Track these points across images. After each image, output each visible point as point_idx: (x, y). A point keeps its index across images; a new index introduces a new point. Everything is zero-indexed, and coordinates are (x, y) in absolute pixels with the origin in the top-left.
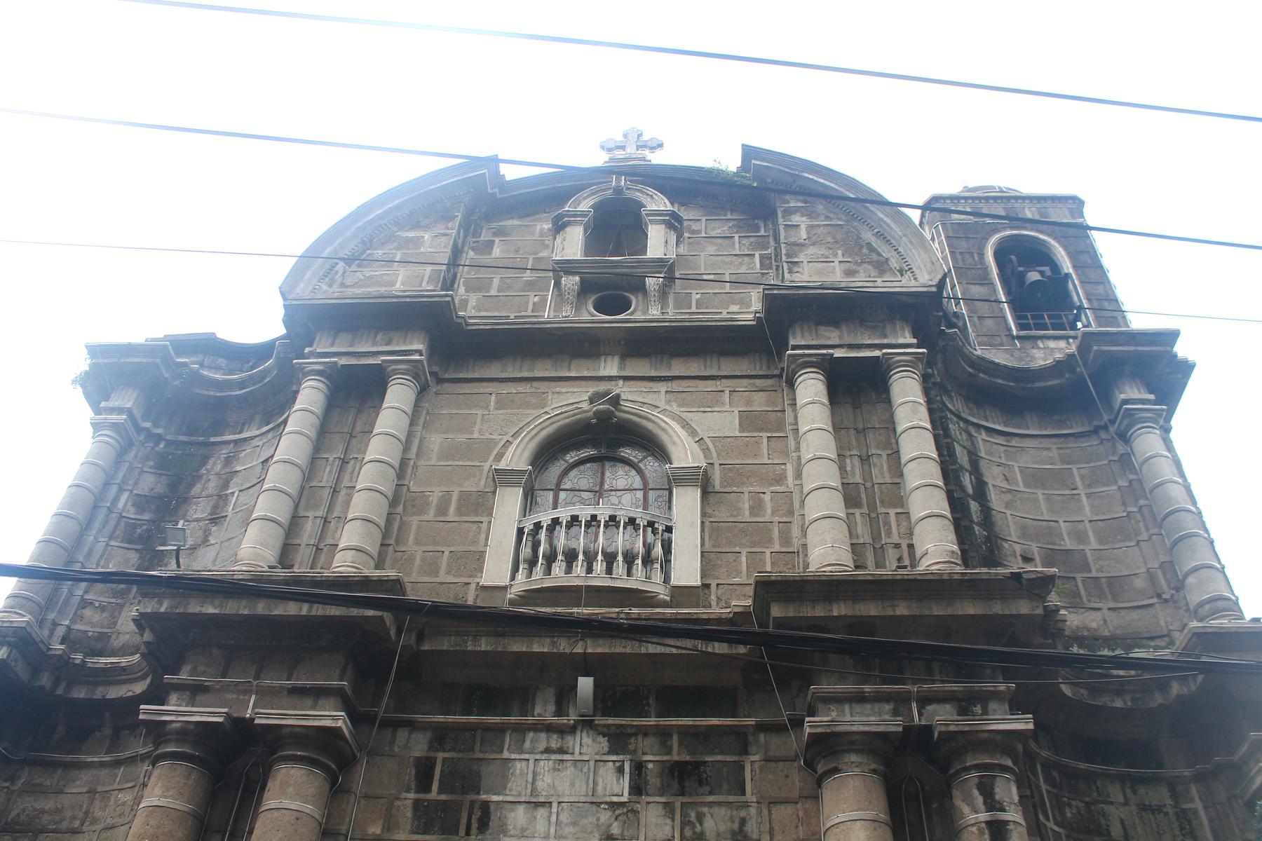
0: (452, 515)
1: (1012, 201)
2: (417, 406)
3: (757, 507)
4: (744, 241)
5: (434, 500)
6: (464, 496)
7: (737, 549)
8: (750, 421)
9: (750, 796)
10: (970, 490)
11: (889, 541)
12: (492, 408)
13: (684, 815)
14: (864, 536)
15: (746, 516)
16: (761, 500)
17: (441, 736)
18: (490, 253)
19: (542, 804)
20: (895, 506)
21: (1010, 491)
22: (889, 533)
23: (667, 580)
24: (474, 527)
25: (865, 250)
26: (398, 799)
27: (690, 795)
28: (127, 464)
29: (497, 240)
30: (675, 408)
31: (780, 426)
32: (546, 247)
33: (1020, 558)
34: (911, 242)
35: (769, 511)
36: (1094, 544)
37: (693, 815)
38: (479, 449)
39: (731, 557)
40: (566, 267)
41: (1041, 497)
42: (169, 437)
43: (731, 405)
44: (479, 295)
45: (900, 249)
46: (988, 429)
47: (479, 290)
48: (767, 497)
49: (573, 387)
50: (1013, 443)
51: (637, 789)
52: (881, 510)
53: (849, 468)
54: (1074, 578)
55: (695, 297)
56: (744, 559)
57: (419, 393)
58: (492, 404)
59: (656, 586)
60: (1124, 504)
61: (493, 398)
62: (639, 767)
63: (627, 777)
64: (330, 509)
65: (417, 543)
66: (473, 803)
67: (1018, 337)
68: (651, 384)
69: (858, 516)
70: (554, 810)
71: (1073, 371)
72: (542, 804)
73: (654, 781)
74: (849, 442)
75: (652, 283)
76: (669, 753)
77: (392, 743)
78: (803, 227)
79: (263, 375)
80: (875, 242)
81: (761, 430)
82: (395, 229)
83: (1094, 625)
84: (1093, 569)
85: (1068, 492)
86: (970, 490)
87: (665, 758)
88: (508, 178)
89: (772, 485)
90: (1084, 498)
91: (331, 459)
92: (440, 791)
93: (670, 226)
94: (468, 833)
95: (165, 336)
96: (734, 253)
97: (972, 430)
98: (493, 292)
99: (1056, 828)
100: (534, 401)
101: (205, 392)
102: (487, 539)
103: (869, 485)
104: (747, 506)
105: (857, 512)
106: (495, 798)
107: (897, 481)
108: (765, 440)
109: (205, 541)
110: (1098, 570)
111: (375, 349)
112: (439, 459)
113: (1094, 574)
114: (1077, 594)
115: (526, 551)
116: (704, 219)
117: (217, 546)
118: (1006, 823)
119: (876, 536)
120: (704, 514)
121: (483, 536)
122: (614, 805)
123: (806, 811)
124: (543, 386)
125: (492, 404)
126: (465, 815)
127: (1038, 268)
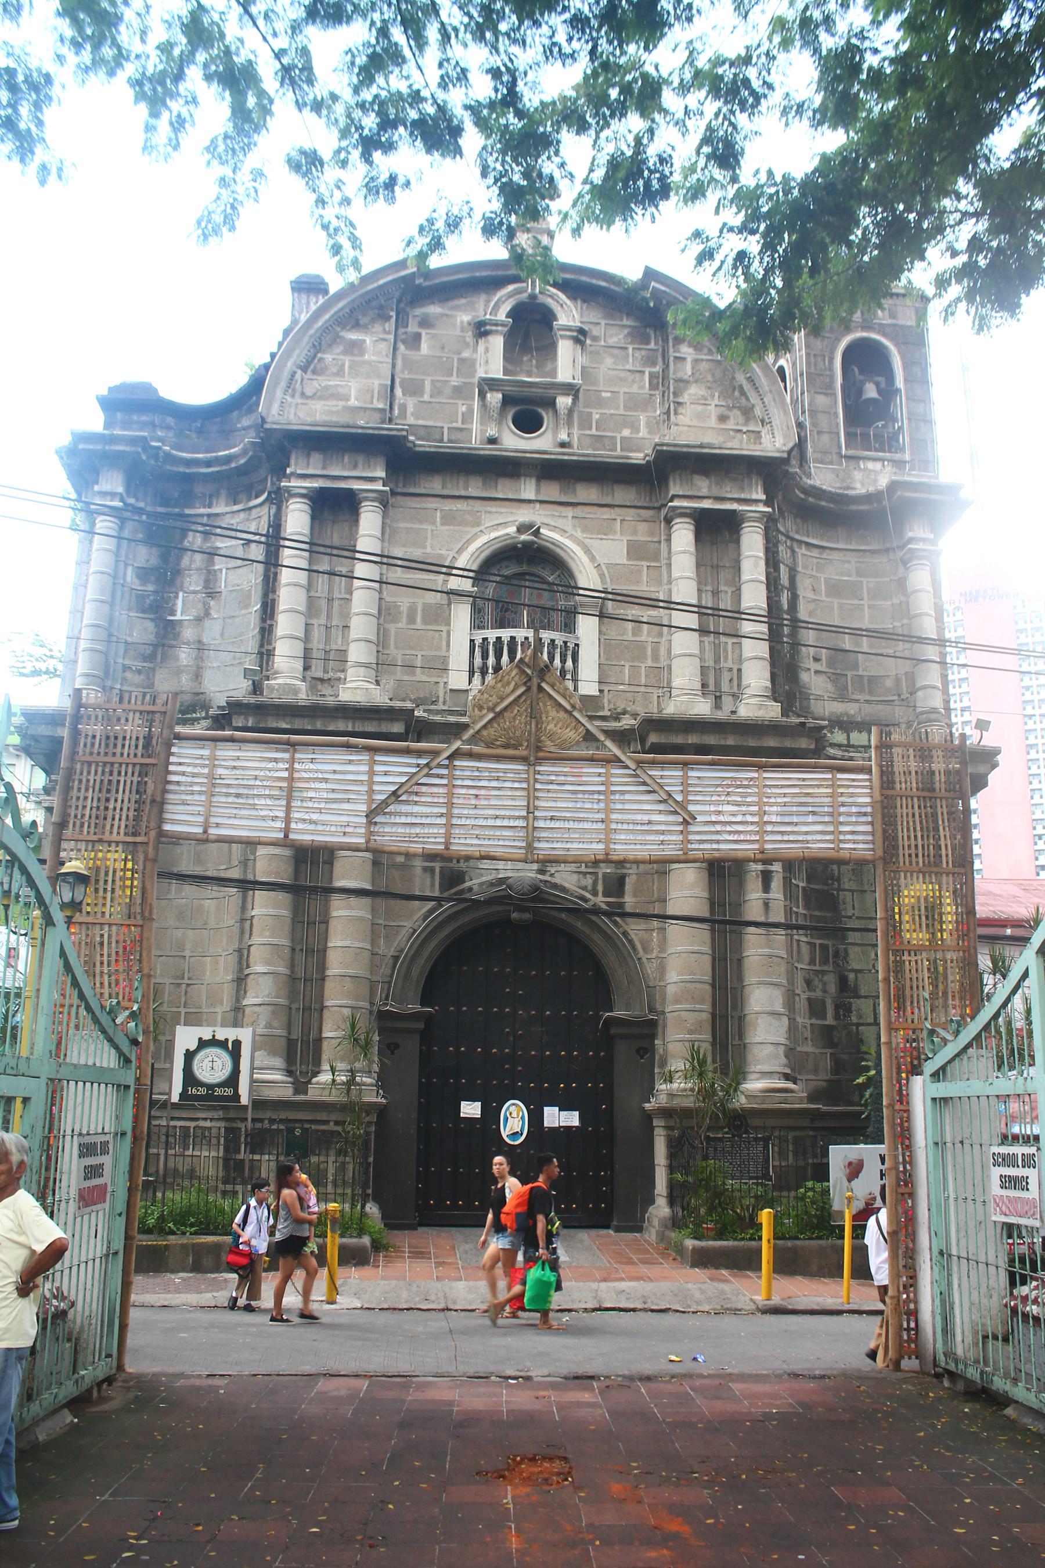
0: (419, 625)
4: (637, 354)
8: (635, 551)
14: (710, 663)
21: (814, 601)
22: (726, 658)
24: (437, 635)
25: (737, 393)
29: (423, 332)
30: (579, 534)
31: (656, 557)
32: (467, 345)
40: (490, 384)
46: (807, 544)
50: (824, 556)
55: (596, 417)
61: (438, 514)
64: (329, 617)
67: (846, 457)
71: (880, 502)
75: (564, 402)
78: (689, 360)
79: (229, 459)
80: (747, 387)
81: (641, 559)
83: (852, 712)
85: (856, 602)
86: (786, 607)
93: (577, 341)
95: (111, 390)
96: (627, 367)
97: (795, 545)
98: (426, 397)
100: (470, 519)
101: (175, 469)
102: (448, 645)
109: (207, 614)
111: (345, 474)
113: (860, 673)
114: (846, 688)
116: (603, 322)
117: (221, 621)
119: (717, 660)
120: (600, 632)
121: (444, 643)
124: (477, 505)
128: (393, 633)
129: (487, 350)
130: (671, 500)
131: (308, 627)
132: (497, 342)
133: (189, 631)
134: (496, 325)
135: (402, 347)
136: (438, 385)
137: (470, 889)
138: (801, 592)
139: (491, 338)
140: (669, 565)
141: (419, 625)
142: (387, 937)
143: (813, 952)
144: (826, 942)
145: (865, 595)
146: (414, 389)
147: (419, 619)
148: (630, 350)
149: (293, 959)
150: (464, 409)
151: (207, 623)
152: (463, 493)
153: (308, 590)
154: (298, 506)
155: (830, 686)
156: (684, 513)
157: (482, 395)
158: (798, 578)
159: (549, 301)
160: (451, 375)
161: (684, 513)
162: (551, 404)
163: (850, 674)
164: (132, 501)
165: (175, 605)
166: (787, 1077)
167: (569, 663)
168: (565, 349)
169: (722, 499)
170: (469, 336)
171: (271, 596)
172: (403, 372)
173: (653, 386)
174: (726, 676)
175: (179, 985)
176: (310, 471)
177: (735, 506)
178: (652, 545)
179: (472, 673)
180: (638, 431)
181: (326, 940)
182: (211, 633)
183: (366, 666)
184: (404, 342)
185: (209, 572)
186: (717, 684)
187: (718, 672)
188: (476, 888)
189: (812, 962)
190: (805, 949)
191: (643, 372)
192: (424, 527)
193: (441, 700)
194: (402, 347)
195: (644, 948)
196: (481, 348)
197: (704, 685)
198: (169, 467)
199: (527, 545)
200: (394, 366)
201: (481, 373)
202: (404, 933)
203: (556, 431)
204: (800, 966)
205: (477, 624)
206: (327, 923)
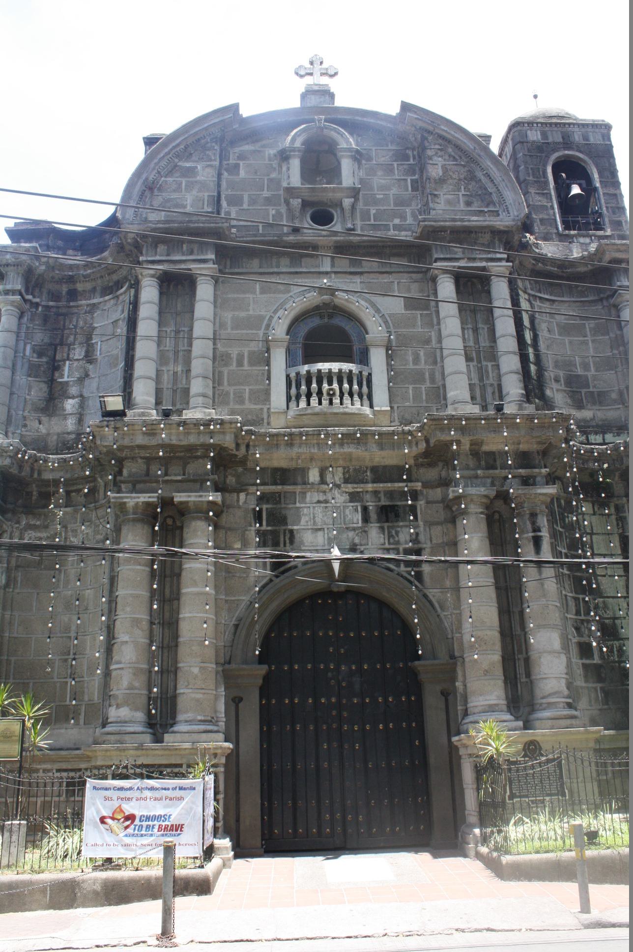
0: (246, 367)
2: (215, 296)
3: (416, 360)
5: (234, 356)
7: (407, 386)
8: (411, 303)
9: (421, 523)
10: (529, 342)
11: (488, 382)
12: (258, 292)
13: (389, 533)
14: (475, 381)
15: (411, 366)
18: (239, 175)
19: (320, 529)
20: (491, 361)
22: (488, 377)
23: (371, 406)
26: (246, 530)
27: (392, 522)
28: (25, 326)
29: (241, 163)
33: (553, 380)
34: (506, 186)
35: (423, 362)
37: (393, 532)
38: (254, 322)
39: (404, 390)
41: (567, 341)
42: (43, 303)
44: (237, 208)
45: (499, 188)
46: (540, 298)
47: (235, 205)
48: (422, 353)
49: (305, 278)
50: (554, 307)
51: (366, 519)
52: (484, 363)
53: (466, 336)
54: (581, 392)
55: (373, 212)
56: (411, 392)
57: (215, 286)
58: (258, 290)
60: (611, 348)
62: (365, 509)
63: (360, 514)
65: (229, 385)
66: (285, 530)
68: (351, 277)
69: (471, 366)
70: (326, 532)
72: (320, 529)
73: (373, 516)
74: (467, 319)
75: (347, 202)
76: (380, 501)
77: (238, 501)
78: (440, 165)
81: (416, 309)
82: (176, 160)
84: (591, 387)
86: (529, 342)
87: (377, 504)
89: (424, 345)
90: (590, 344)
91: (168, 331)
92: (268, 525)
94: (285, 545)
98: (245, 206)
99: (561, 530)
103: (477, 346)
104: (411, 358)
105: (471, 364)
106: (295, 527)
107: (493, 345)
108: (419, 316)
109: (87, 375)
110: (594, 387)
111: (184, 258)
112: (232, 329)
113: (591, 389)
115: (293, 391)
116: (374, 148)
117: (97, 379)
118: (541, 537)
119: (481, 379)
122: (354, 529)
123: (447, 529)
125: (258, 290)
129: (288, 169)
130: (435, 262)
131: (159, 373)
132: (295, 164)
133: (74, 388)
135: (226, 174)
137: (295, 567)
138: (540, 334)
139: (291, 161)
140: (438, 312)
141: (246, 367)
142: (229, 610)
143: (577, 606)
145: (588, 333)
146: (235, 201)
148: (396, 166)
149: (151, 631)
150: (274, 212)
151: (87, 382)
152: (276, 270)
153: (159, 345)
154: (149, 282)
156: (446, 271)
157: (287, 203)
158: (537, 321)
159: (334, 134)
160: (263, 190)
161: (446, 271)
163: (583, 391)
164: (29, 297)
165: (63, 370)
166: (570, 706)
167: (365, 389)
168: (347, 166)
169: (474, 259)
170: (275, 164)
171: (131, 352)
172: (227, 190)
173: (414, 189)
174: (489, 390)
175: (66, 660)
176: (158, 258)
177: (484, 264)
179: (289, 399)
180: (405, 219)
181: (178, 613)
182: (91, 388)
183: (204, 396)
184: (227, 170)
185: (88, 345)
186: (483, 398)
187: (483, 388)
188: (300, 565)
189: (578, 613)
190: (572, 603)
191: (406, 180)
192: (247, 296)
194: (226, 174)
195: (442, 608)
196: (284, 169)
197: (473, 398)
199: (326, 305)
200: (219, 185)
201: (285, 184)
202: (243, 606)
203: (344, 220)
204: (569, 616)
205: (291, 362)
206: (178, 599)
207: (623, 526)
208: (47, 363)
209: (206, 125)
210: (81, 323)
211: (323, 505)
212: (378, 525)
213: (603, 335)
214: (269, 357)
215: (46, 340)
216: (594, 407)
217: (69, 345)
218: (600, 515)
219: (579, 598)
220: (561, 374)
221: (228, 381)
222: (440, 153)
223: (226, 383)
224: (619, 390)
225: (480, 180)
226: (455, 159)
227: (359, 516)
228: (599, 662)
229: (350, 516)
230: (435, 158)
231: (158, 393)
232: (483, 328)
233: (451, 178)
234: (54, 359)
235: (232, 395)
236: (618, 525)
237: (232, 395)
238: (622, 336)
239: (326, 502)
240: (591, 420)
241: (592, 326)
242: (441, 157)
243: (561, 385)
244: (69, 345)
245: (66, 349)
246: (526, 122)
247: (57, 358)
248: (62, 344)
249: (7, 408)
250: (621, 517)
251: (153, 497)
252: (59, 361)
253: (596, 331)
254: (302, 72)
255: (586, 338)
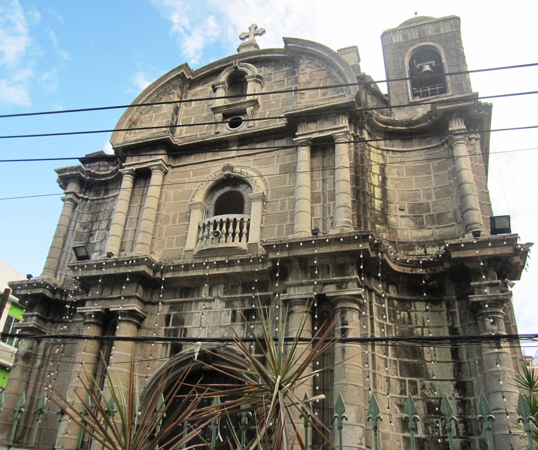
1: (423, 26)
5: (171, 218)
6: (181, 214)
12: (191, 176)
16: (284, 203)
17: (174, 306)
21: (399, 179)
22: (329, 212)
30: (256, 167)
35: (287, 207)
36: (434, 199)
41: (413, 179)
43: (277, 163)
46: (393, 151)
48: (287, 202)
51: (234, 320)
54: (422, 216)
59: (243, 245)
60: (449, 179)
61: (191, 172)
62: (234, 312)
63: (230, 316)
65: (165, 236)
66: (182, 329)
73: (239, 317)
76: (244, 306)
85: (426, 176)
88: (195, 70)
92: (173, 325)
93: (257, 81)
95: (86, 155)
97: (385, 153)
100: (205, 171)
106: (188, 326)
108: (288, 176)
111: (146, 161)
113: (431, 213)
114: (423, 223)
116: (273, 72)
119: (324, 215)
126: (179, 333)
127: (429, 63)
128: (165, 229)
134: (219, 84)
136: (197, 118)
144: (414, 379)
147: (177, 221)
155: (412, 223)
158: (387, 169)
159: (244, 69)
162: (244, 113)
163: (424, 215)
177: (330, 133)
178: (293, 164)
189: (403, 392)
193: (182, 257)
198: (97, 179)
207: (452, 320)
208: (87, 232)
209: (168, 80)
210: (108, 208)
211: (208, 311)
212: (241, 323)
213: (444, 170)
214: (190, 216)
215: (89, 220)
216: (433, 227)
217: (100, 221)
218: (432, 311)
219: (405, 380)
220: (406, 205)
221: (165, 234)
222: (309, 65)
223: (164, 234)
224: (454, 210)
225: (335, 77)
226: (319, 66)
227: (230, 318)
228: (423, 436)
229: (224, 318)
230: (306, 69)
231: (122, 243)
232: (330, 178)
233: (315, 80)
234: (91, 231)
235: (166, 242)
236: (448, 319)
237: (166, 242)
238: (455, 168)
239: (210, 308)
240: (430, 236)
241: (435, 165)
242: (310, 67)
243: (405, 212)
244: (100, 221)
245: (98, 224)
246: (391, 32)
247: (93, 229)
248: (96, 221)
249: (57, 261)
250: (451, 312)
251: (99, 308)
252: (94, 231)
253: (438, 169)
254: (243, 37)
255: (430, 175)
